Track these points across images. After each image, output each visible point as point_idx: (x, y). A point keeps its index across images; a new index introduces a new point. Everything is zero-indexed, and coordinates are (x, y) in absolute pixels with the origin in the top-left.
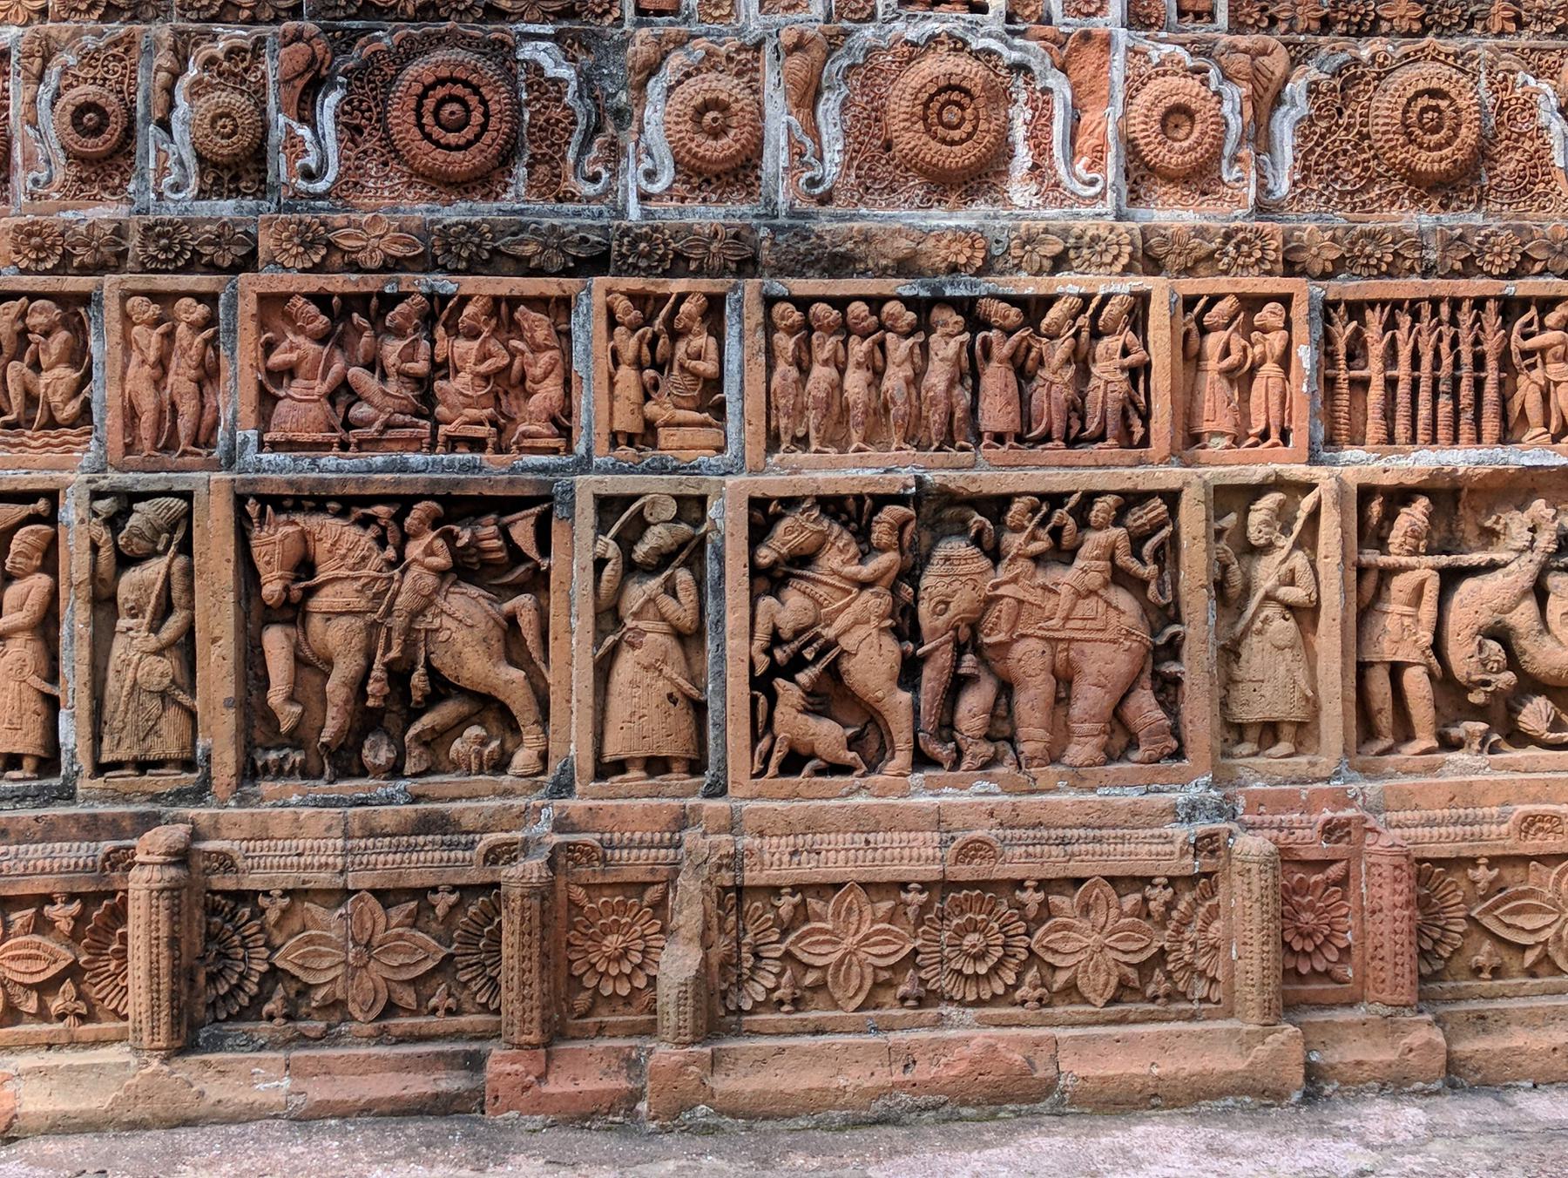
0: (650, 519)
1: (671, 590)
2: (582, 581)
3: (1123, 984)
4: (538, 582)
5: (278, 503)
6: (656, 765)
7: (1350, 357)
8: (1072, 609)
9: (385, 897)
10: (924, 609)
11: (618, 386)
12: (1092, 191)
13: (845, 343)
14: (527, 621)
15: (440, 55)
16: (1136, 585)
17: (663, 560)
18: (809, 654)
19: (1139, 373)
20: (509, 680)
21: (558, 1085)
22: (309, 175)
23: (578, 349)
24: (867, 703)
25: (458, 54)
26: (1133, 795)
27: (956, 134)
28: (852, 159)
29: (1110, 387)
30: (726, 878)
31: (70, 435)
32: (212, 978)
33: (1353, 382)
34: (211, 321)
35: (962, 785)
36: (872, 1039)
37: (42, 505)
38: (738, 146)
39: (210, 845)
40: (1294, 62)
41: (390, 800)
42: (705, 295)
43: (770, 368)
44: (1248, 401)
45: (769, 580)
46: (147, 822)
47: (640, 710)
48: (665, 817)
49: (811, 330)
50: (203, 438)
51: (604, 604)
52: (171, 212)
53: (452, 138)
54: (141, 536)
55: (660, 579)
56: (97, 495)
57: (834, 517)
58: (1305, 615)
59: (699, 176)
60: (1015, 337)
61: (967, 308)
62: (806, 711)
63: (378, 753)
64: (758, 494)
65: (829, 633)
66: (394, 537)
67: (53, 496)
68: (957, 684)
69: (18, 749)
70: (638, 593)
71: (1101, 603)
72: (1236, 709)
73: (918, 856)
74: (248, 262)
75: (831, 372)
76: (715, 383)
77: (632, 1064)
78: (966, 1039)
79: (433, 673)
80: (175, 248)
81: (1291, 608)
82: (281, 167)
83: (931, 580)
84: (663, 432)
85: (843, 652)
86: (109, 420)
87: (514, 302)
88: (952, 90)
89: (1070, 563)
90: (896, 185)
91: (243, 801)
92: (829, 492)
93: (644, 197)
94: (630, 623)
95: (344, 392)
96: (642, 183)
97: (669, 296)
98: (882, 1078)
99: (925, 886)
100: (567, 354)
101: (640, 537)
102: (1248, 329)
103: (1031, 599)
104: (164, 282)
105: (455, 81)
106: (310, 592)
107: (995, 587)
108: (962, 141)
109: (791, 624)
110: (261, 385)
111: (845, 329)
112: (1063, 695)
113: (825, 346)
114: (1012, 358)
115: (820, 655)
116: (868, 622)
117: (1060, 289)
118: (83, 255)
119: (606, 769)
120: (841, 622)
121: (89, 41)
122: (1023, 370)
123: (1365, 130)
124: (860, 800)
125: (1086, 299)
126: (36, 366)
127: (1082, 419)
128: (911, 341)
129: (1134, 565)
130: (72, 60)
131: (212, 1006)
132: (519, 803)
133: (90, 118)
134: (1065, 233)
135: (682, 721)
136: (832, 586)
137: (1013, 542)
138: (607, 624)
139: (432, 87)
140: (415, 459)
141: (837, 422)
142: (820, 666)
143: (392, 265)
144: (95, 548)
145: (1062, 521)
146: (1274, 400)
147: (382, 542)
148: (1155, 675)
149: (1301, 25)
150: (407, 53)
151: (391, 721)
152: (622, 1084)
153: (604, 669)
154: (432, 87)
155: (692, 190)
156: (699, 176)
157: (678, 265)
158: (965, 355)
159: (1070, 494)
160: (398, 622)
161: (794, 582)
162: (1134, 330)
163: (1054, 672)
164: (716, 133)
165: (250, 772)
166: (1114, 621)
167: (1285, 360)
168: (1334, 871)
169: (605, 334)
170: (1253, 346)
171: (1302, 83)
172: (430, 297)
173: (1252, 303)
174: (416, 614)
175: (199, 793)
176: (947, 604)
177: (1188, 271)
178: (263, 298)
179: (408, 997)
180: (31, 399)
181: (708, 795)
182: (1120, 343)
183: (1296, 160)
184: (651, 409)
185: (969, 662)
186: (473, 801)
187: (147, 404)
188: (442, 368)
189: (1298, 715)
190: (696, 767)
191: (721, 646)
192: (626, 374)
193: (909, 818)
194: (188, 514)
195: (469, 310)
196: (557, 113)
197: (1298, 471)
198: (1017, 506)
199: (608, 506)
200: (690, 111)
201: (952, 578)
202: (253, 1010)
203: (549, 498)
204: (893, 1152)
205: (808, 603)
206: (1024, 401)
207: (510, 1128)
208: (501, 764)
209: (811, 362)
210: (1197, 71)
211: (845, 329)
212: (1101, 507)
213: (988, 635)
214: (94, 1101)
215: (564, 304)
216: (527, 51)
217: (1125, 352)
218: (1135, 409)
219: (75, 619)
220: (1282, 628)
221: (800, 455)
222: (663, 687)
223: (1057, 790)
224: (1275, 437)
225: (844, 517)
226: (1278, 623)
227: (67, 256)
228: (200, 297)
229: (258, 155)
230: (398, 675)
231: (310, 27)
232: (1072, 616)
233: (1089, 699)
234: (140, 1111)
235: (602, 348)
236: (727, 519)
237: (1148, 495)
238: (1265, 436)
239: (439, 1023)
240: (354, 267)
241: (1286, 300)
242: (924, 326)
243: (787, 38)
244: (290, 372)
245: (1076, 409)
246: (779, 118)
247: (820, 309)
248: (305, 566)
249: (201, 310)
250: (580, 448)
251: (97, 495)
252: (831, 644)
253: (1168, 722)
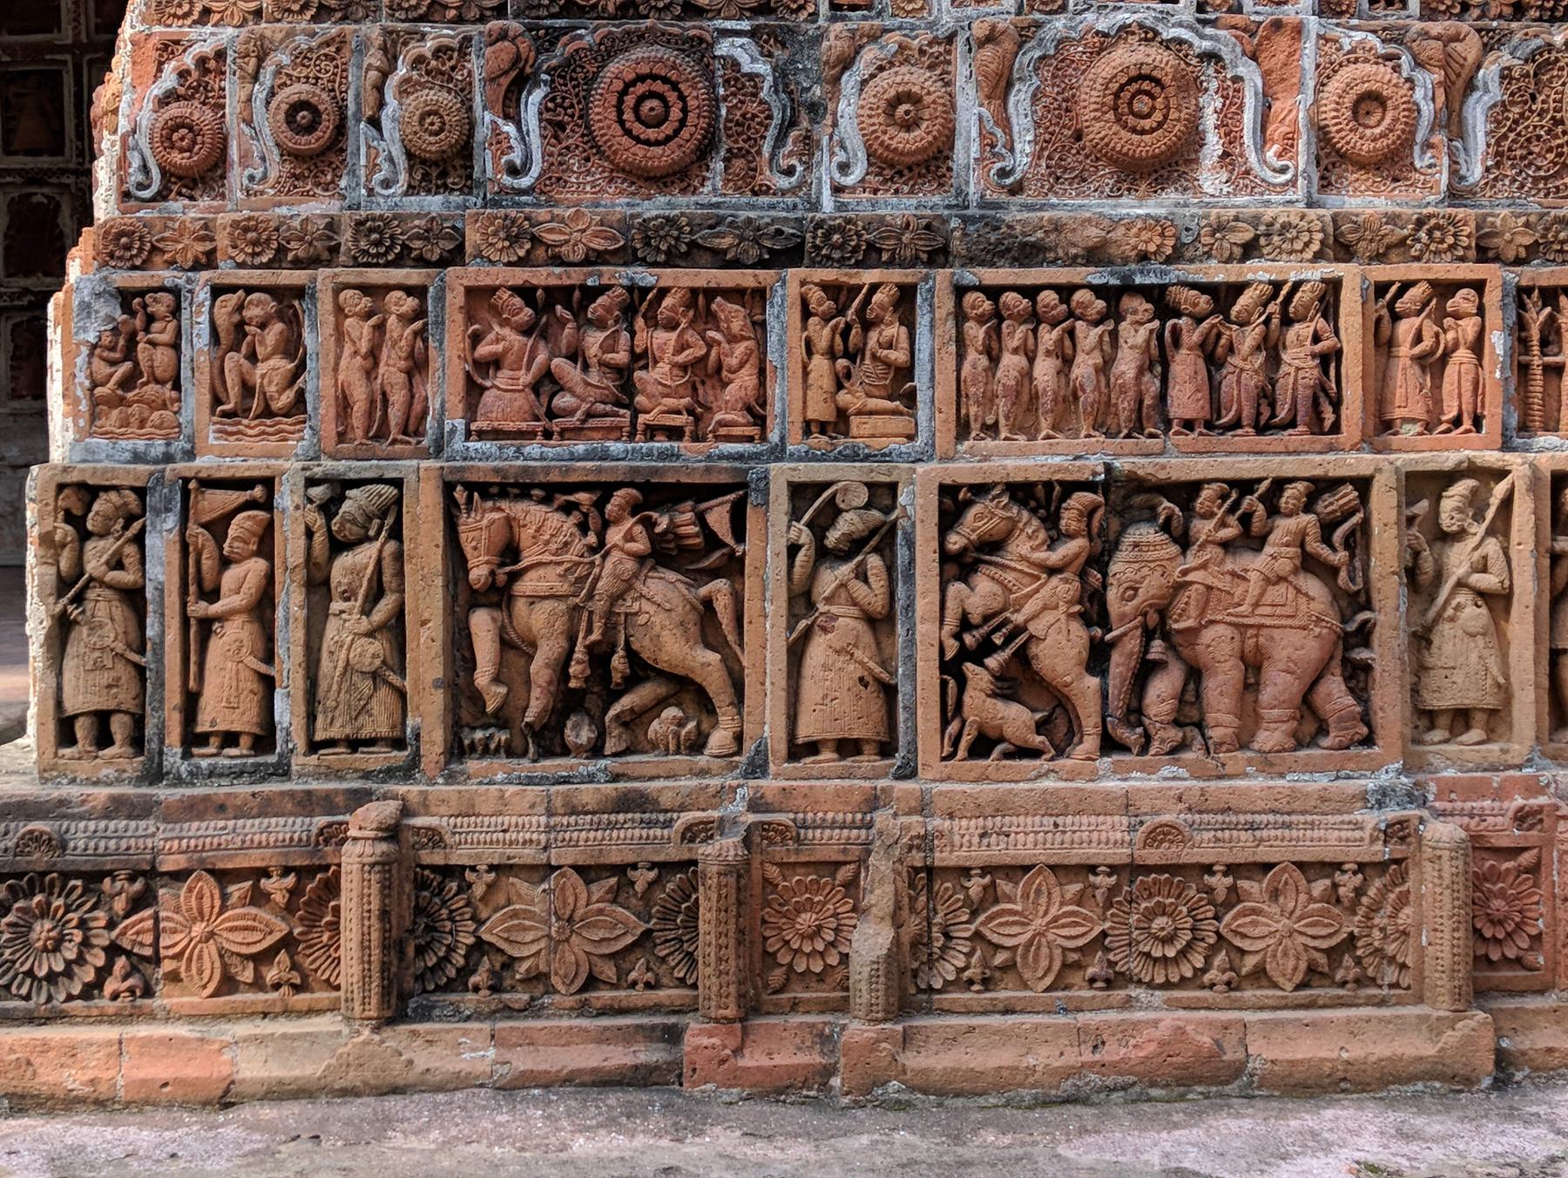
0: (842, 506)
1: (862, 575)
2: (776, 566)
3: (1312, 970)
4: (733, 567)
5: (483, 490)
6: (848, 747)
7: (1544, 343)
8: (1262, 595)
9: (587, 872)
10: (1112, 595)
11: (812, 376)
12: (1283, 178)
13: (1035, 331)
14: (722, 605)
15: (639, 52)
16: (1327, 572)
17: (854, 546)
18: (998, 639)
19: (1329, 360)
20: (705, 663)
21: (752, 1059)
22: (513, 171)
23: (773, 339)
24: (1055, 687)
25: (658, 52)
26: (1322, 781)
27: (1147, 124)
28: (1042, 149)
29: (1301, 374)
30: (917, 859)
31: (286, 424)
32: (421, 951)
33: (1547, 368)
34: (420, 313)
35: (1150, 770)
36: (1061, 1019)
37: (258, 491)
38: (930, 138)
39: (419, 821)
40: (1487, 48)
41: (591, 778)
42: (897, 285)
43: (960, 357)
44: (1440, 387)
45: (958, 566)
46: (359, 798)
47: (833, 692)
48: (857, 797)
49: (1001, 319)
50: (412, 427)
51: (797, 589)
52: (381, 208)
53: (652, 134)
54: (354, 522)
55: (852, 565)
56: (311, 482)
57: (1023, 503)
58: (1498, 601)
59: (892, 168)
60: (1205, 325)
61: (1157, 296)
62: (994, 695)
63: (579, 733)
64: (948, 481)
65: (1018, 618)
66: (594, 524)
67: (268, 483)
68: (1145, 670)
69: (236, 727)
70: (830, 578)
71: (1291, 589)
72: (1426, 695)
73: (1107, 839)
74: (456, 256)
75: (1020, 361)
76: (906, 372)
77: (825, 1040)
78: (1155, 1021)
79: (632, 655)
80: (385, 242)
81: (1483, 595)
82: (486, 164)
83: (1119, 567)
84: (854, 420)
85: (1031, 637)
86: (322, 410)
87: (711, 293)
88: (1142, 80)
89: (1259, 549)
90: (1086, 174)
91: (451, 778)
92: (1019, 479)
93: (837, 190)
94: (822, 607)
95: (547, 383)
96: (835, 176)
97: (861, 287)
98: (1071, 1058)
99: (1113, 869)
100: (762, 344)
101: (832, 523)
102: (1440, 316)
103: (1220, 585)
104: (375, 276)
105: (654, 77)
106: (515, 577)
107: (1185, 573)
108: (1153, 130)
109: (980, 610)
110: (468, 376)
111: (1035, 318)
112: (1252, 681)
113: (1015, 335)
114: (1202, 345)
115: (1009, 639)
116: (1056, 607)
117: (1250, 276)
118: (297, 249)
119: (799, 750)
120: (1030, 608)
121: (302, 41)
122: (1213, 357)
123: (1558, 116)
124: (1049, 784)
125: (1277, 286)
126: (253, 357)
127: (1272, 405)
129: (1324, 551)
130: (286, 59)
131: (420, 978)
132: (715, 782)
133: (303, 116)
134: (1255, 220)
135: (873, 703)
136: (1021, 571)
137: (1203, 528)
138: (800, 608)
139: (633, 83)
140: (616, 447)
141: (1026, 410)
142: (1008, 652)
143: (594, 259)
144: (309, 534)
145: (1252, 507)
146: (1467, 386)
147: (583, 528)
148: (1346, 661)
149: (1494, 11)
150: (608, 50)
151: (592, 702)
152: (816, 1058)
153: (796, 653)
154: (633, 83)
155: (885, 181)
156: (892, 168)
157: (870, 255)
158: (1154, 342)
159: (1260, 480)
160: (599, 605)
161: (983, 568)
162: (1325, 316)
163: (1242, 658)
164: (908, 126)
165: (457, 750)
166: (1303, 608)
167: (1478, 346)
168: (1526, 858)
169: (799, 324)
170: (1445, 332)
171: (1495, 68)
172: (630, 289)
173: (1444, 289)
174: (616, 598)
175: (408, 771)
176: (1136, 590)
177: (1380, 258)
178: (470, 292)
179: (608, 971)
180: (247, 389)
181: (898, 778)
182: (1311, 330)
183: (1488, 146)
184: (843, 397)
185: (1157, 648)
186: (670, 780)
187: (359, 395)
188: (641, 358)
189: (1491, 702)
190: (886, 749)
191: (911, 631)
192: (819, 363)
193: (1099, 803)
194: (399, 501)
195: (668, 301)
196: (753, 107)
197: (1491, 457)
198: (1207, 492)
199: (801, 493)
200: (883, 104)
201: (1141, 563)
202: (459, 982)
203: (744, 485)
204: (1083, 1131)
205: (997, 588)
206: (1214, 388)
207: (706, 1100)
208: (697, 745)
209: (1000, 350)
210: (1388, 58)
211: (1035, 318)
212: (1291, 495)
213: (1176, 621)
214: (308, 1069)
215: (759, 296)
216: (724, 48)
217: (1316, 339)
218: (1326, 396)
219: (291, 602)
220: (1474, 614)
221: (989, 443)
222: (855, 671)
223: (1245, 775)
224: (1467, 424)
225: (1033, 504)
226: (1470, 610)
227: (281, 250)
228: (409, 290)
229: (465, 151)
230: (599, 657)
231: (514, 25)
232: (1263, 602)
233: (1278, 685)
234: (352, 1078)
235: (796, 339)
236: (917, 505)
237: (1340, 482)
238: (1457, 422)
239: (638, 996)
240: (558, 260)
241: (1479, 286)
242: (1114, 313)
243: (980, 30)
244: (495, 363)
245: (1267, 395)
246: (970, 110)
247: (1010, 298)
248: (510, 552)
249: (410, 303)
250: (774, 436)
251: (311, 482)
252: (1019, 630)
253: (1358, 709)
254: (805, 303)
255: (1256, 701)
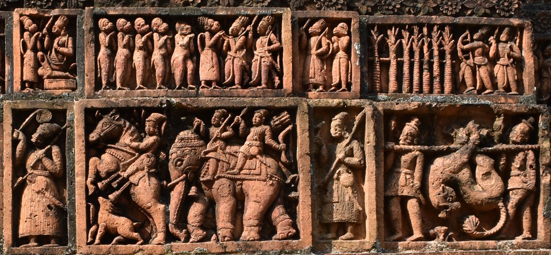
0: (39, 121)
1: (49, 154)
11: (25, 60)
13: (134, 38)
17: (45, 141)
19: (277, 53)
24: (143, 209)
29: (263, 60)
42: (67, 16)
44: (331, 71)
45: (94, 149)
49: (117, 32)
55: (43, 150)
62: (113, 213)
72: (325, 216)
75: (125, 51)
76: (71, 58)
84: (46, 82)
85: (131, 184)
89: (242, 144)
94: (30, 171)
102: (330, 35)
103: (224, 159)
107: (206, 153)
109: (105, 170)
115: (120, 185)
116: (143, 169)
125: (251, 17)
128: (165, 37)
129: (274, 144)
136: (126, 152)
137: (215, 131)
146: (343, 69)
158: (192, 44)
162: (274, 33)
166: (264, 171)
167: (348, 50)
169: (19, 35)
170: (333, 43)
176: (182, 161)
182: (268, 39)
192: (29, 54)
213: (203, 177)
217: (270, 43)
218: (274, 71)
233: (252, 209)
241: (348, 21)
242: (171, 31)
247: (121, 21)
252: (126, 180)
253: (291, 220)
254: (22, 24)
255: (242, 218)
